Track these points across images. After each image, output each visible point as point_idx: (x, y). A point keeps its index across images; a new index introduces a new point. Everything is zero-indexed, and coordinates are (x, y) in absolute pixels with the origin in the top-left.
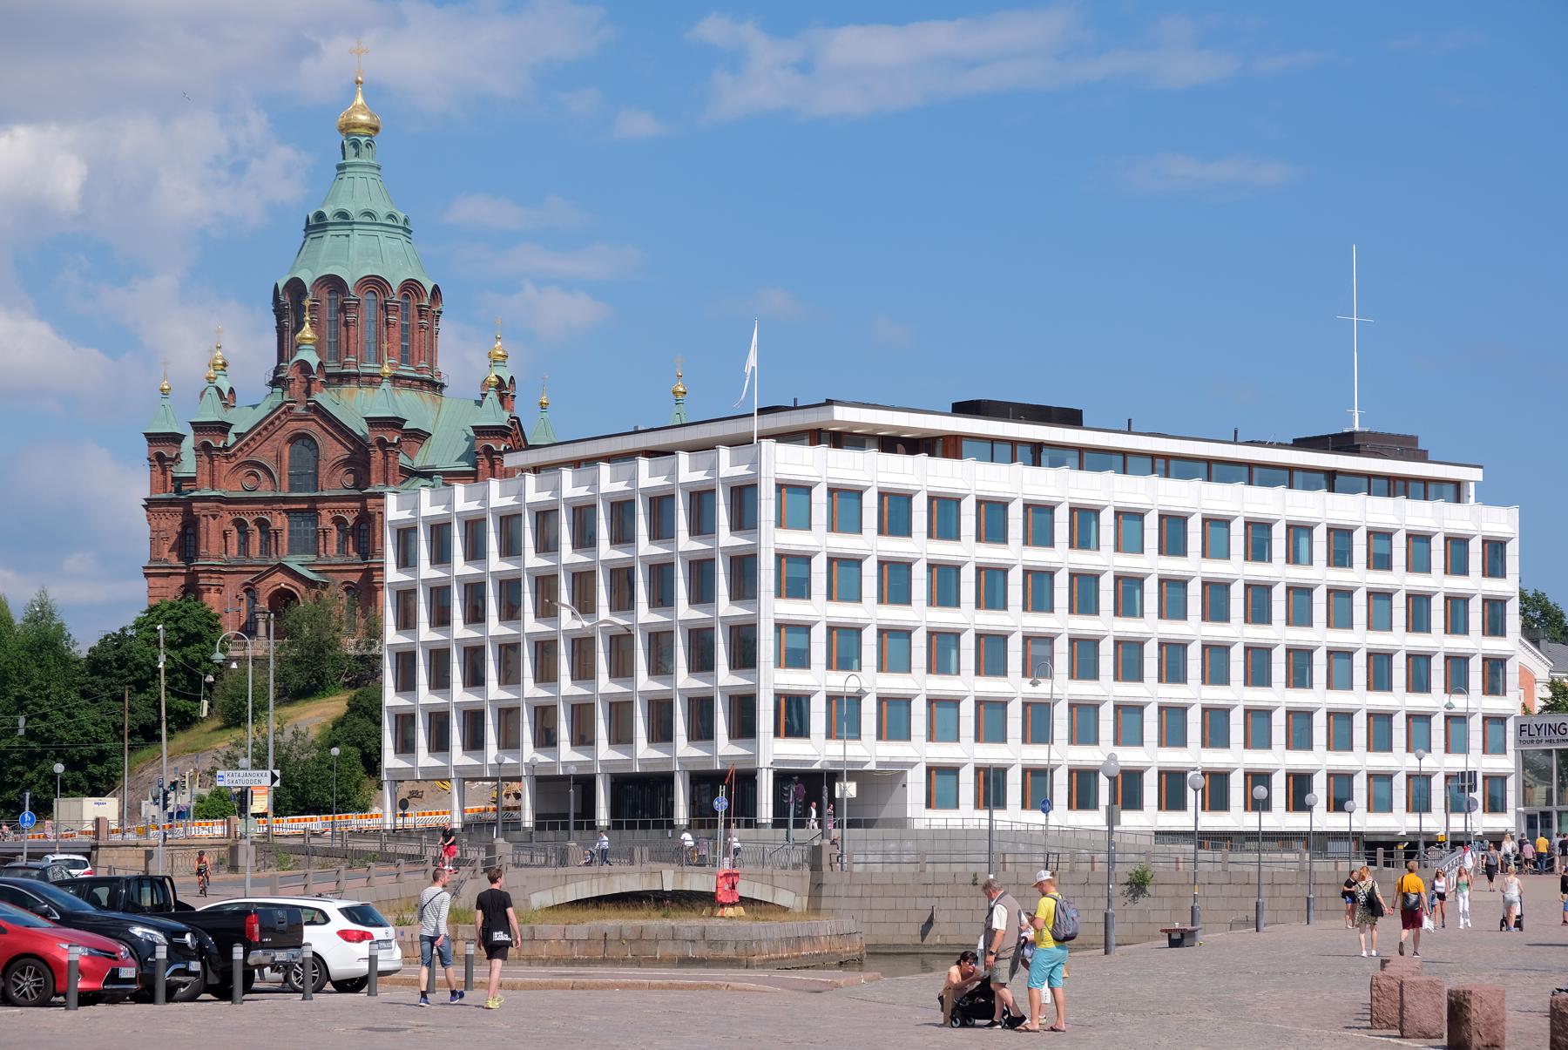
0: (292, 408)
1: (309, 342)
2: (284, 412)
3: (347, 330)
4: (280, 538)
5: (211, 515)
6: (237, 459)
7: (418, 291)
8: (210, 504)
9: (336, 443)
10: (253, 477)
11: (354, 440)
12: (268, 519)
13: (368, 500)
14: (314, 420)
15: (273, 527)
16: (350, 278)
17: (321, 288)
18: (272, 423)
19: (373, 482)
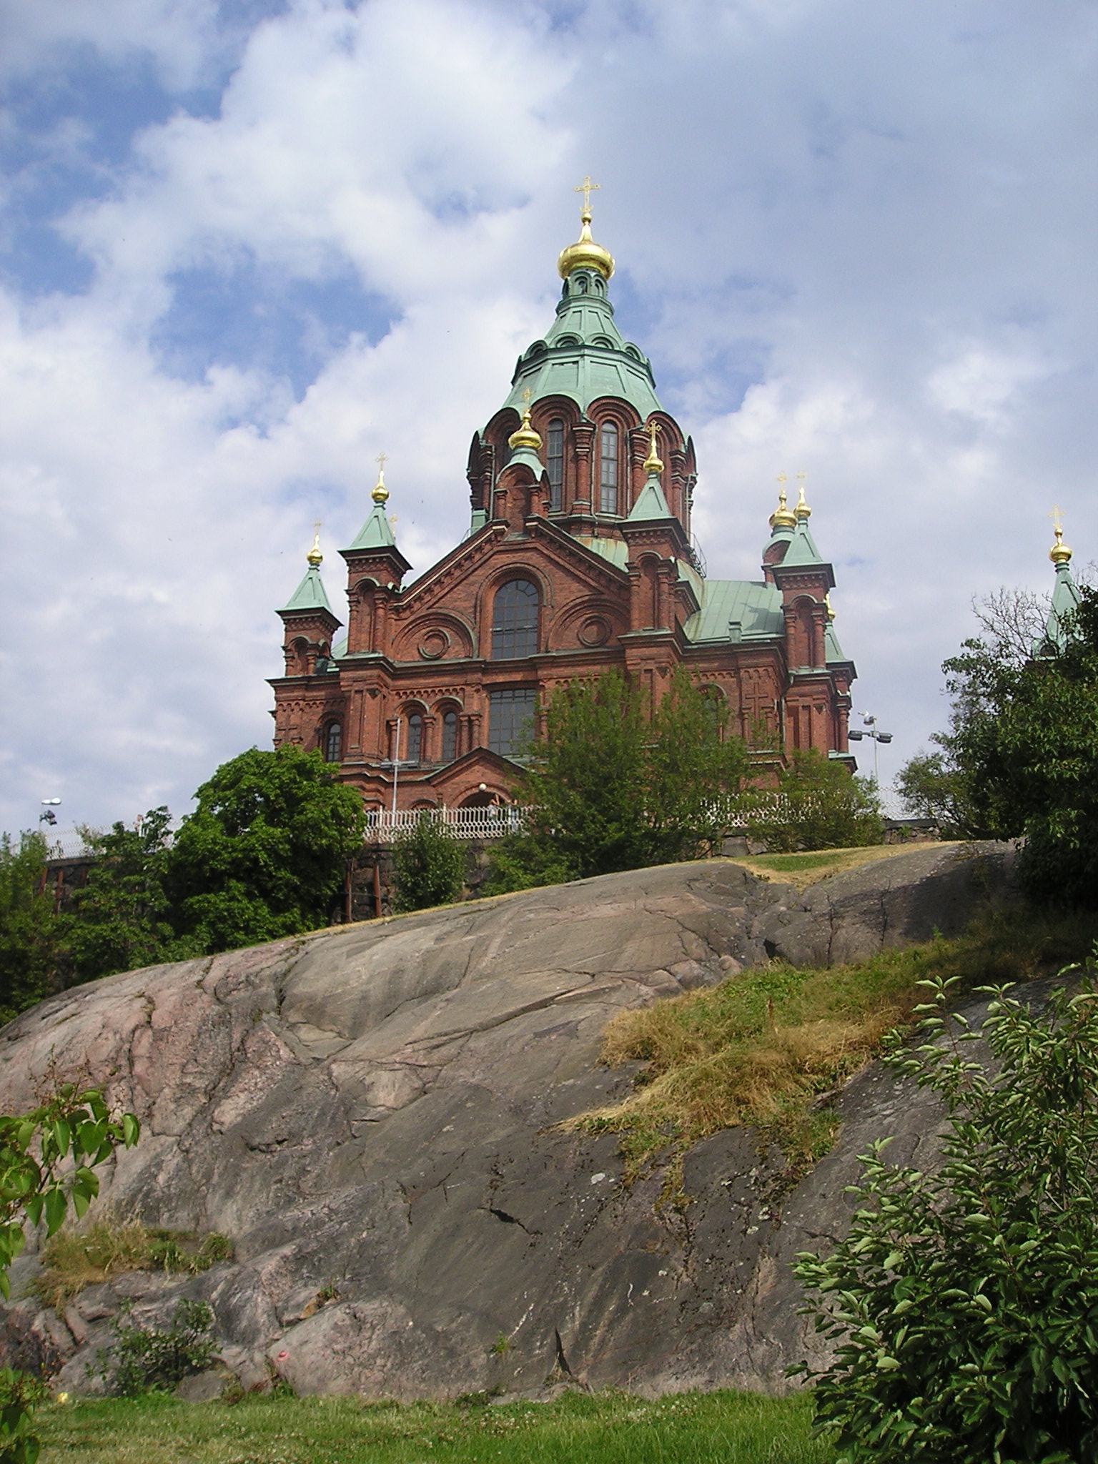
0: (502, 533)
1: (529, 443)
2: (489, 541)
3: (577, 468)
4: (476, 729)
5: (368, 690)
6: (412, 613)
7: (672, 434)
8: (368, 673)
9: (569, 580)
10: (436, 641)
11: (601, 573)
12: (458, 699)
13: (628, 652)
14: (535, 549)
15: (467, 711)
16: (583, 400)
17: (541, 416)
18: (469, 557)
19: (635, 623)
